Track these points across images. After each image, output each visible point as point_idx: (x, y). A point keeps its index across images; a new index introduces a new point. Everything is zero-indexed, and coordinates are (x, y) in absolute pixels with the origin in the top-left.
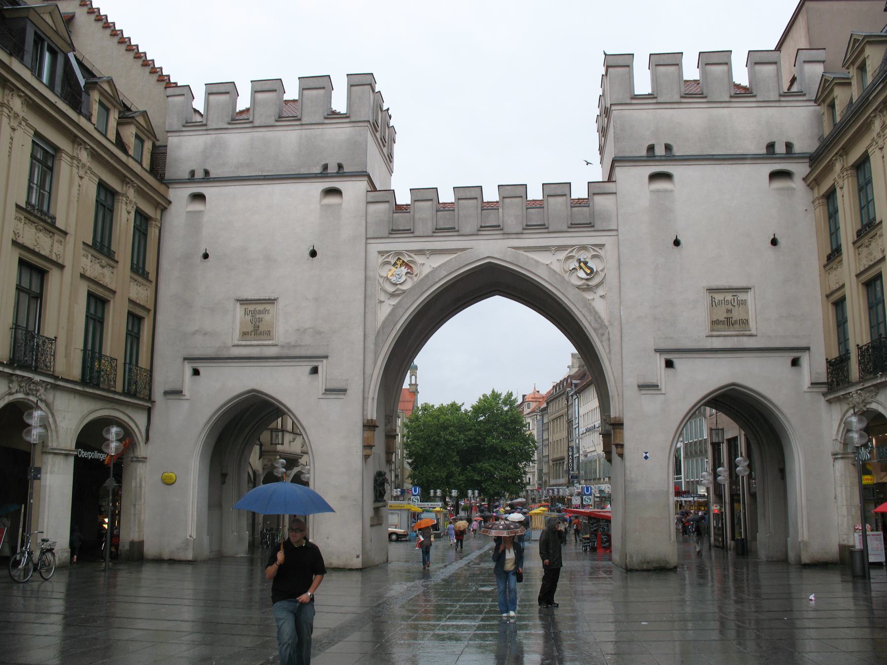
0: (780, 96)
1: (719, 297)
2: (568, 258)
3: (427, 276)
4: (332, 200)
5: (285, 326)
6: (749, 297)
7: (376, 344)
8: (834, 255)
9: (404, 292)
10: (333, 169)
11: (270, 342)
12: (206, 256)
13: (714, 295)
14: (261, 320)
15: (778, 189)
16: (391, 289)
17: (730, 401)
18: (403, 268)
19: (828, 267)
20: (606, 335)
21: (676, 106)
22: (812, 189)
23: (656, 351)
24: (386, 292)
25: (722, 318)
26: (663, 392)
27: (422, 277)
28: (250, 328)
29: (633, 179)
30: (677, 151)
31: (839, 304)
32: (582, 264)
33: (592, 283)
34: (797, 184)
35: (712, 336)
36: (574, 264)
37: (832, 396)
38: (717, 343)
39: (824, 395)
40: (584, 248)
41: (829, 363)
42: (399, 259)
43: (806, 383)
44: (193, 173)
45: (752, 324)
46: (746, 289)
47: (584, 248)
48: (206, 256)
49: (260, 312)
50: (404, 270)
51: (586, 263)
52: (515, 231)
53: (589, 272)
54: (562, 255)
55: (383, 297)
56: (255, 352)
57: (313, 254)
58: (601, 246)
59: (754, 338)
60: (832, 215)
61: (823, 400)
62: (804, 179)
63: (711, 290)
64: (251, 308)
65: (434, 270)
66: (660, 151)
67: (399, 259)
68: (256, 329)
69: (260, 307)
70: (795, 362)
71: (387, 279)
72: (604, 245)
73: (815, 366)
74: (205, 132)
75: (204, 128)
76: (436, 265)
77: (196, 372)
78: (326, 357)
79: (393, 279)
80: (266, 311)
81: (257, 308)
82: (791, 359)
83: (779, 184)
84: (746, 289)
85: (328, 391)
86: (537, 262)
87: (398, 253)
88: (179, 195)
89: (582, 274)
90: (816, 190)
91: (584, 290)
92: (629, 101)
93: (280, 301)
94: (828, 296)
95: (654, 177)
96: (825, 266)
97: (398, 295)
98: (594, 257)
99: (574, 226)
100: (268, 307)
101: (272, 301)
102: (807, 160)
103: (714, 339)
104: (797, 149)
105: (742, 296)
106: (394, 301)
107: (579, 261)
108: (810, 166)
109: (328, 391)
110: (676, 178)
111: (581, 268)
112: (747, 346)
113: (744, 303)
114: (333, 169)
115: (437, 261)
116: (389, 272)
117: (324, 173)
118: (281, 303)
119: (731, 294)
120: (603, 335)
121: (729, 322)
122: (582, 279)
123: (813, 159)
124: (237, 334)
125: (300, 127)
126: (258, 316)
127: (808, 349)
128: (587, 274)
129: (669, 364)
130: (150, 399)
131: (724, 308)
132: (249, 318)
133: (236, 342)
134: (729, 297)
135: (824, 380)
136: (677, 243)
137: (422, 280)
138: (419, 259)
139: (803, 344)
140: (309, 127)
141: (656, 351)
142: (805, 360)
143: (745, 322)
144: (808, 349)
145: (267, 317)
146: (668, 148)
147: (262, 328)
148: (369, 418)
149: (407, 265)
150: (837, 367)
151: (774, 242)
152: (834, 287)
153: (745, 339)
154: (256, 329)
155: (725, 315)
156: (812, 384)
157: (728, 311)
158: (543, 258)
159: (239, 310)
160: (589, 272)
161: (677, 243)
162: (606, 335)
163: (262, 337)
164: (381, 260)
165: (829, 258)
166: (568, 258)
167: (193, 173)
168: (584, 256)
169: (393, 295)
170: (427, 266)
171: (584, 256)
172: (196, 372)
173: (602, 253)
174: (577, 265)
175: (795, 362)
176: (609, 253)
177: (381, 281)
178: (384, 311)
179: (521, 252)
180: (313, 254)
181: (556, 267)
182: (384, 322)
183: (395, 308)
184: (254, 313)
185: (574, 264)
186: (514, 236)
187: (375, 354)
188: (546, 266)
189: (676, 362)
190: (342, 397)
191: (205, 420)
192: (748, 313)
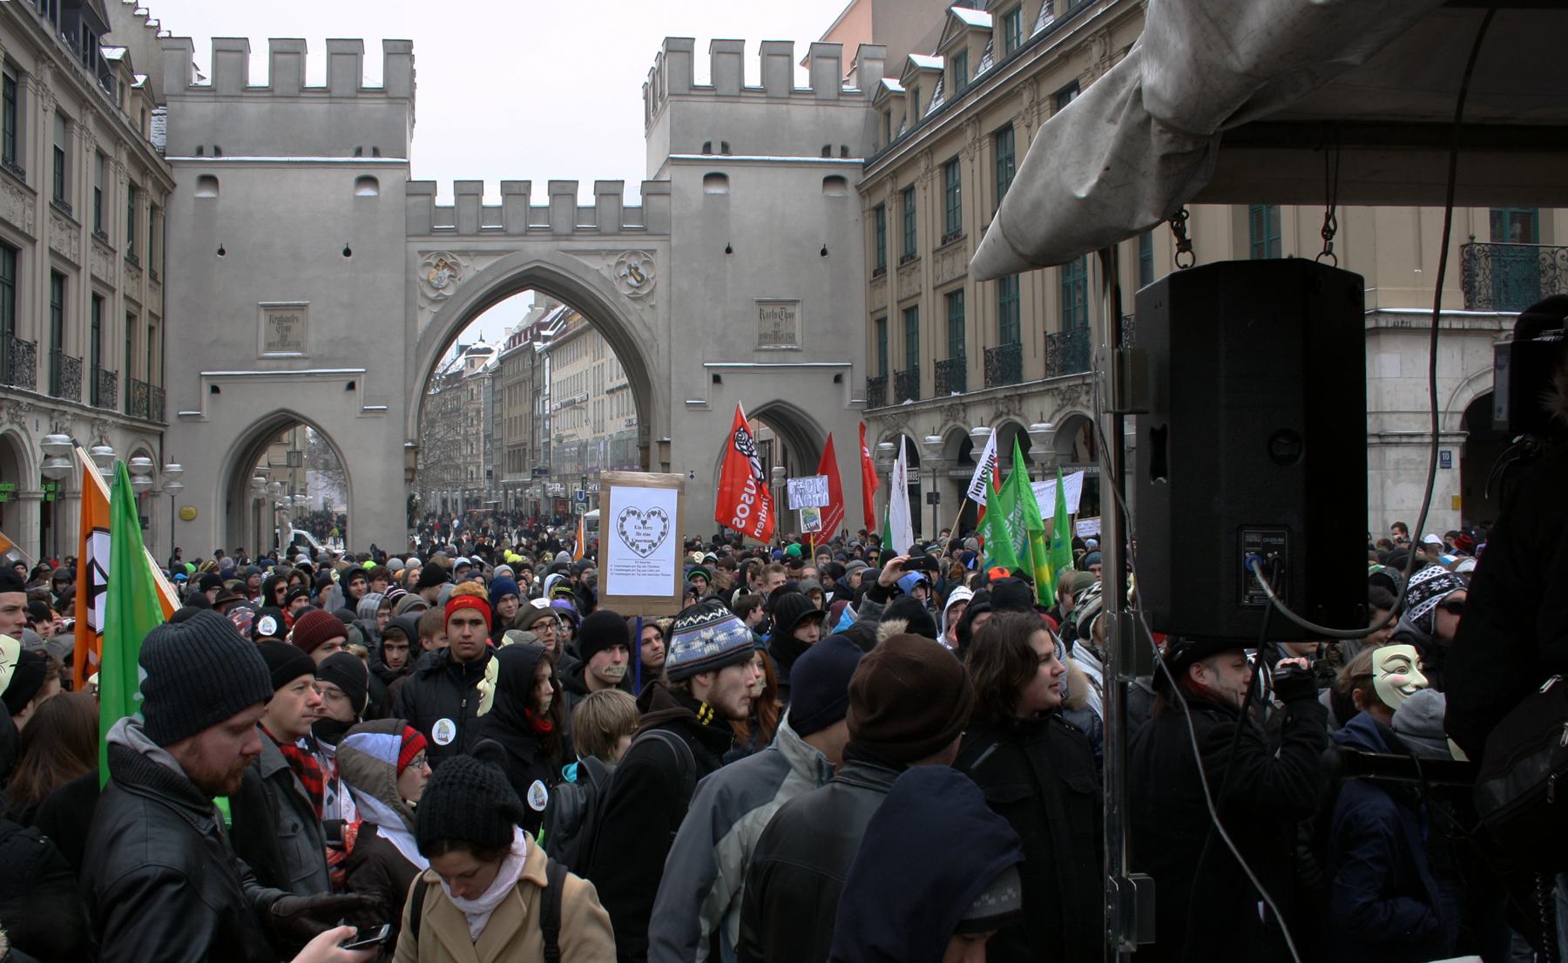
2: (619, 263)
3: (471, 281)
6: (797, 310)
8: (880, 271)
9: (447, 298)
14: (288, 329)
16: (432, 295)
17: (774, 414)
24: (424, 295)
28: (276, 338)
29: (690, 182)
31: (882, 323)
36: (624, 271)
45: (798, 338)
47: (634, 253)
49: (287, 319)
50: (447, 272)
51: (636, 269)
54: (613, 261)
55: (424, 303)
58: (653, 252)
60: (881, 230)
63: (760, 302)
64: (277, 314)
65: (480, 274)
69: (287, 314)
70: (838, 379)
71: (429, 282)
73: (856, 383)
76: (481, 268)
80: (293, 319)
84: (794, 302)
86: (586, 267)
87: (440, 254)
89: (633, 282)
91: (634, 299)
98: (644, 262)
100: (297, 314)
101: (302, 307)
105: (790, 309)
106: (436, 309)
107: (630, 267)
113: (792, 316)
115: (483, 264)
116: (433, 274)
118: (312, 310)
121: (776, 337)
124: (262, 345)
129: (717, 379)
134: (777, 310)
138: (463, 261)
142: (847, 379)
147: (292, 337)
149: (446, 265)
150: (876, 388)
152: (879, 306)
157: (776, 324)
158: (593, 263)
159: (263, 317)
161: (729, 250)
164: (421, 261)
166: (619, 263)
168: (634, 261)
169: (434, 301)
170: (472, 269)
171: (634, 261)
175: (838, 379)
176: (660, 260)
178: (424, 320)
181: (605, 273)
184: (281, 320)
185: (624, 271)
188: (598, 270)
189: (723, 377)
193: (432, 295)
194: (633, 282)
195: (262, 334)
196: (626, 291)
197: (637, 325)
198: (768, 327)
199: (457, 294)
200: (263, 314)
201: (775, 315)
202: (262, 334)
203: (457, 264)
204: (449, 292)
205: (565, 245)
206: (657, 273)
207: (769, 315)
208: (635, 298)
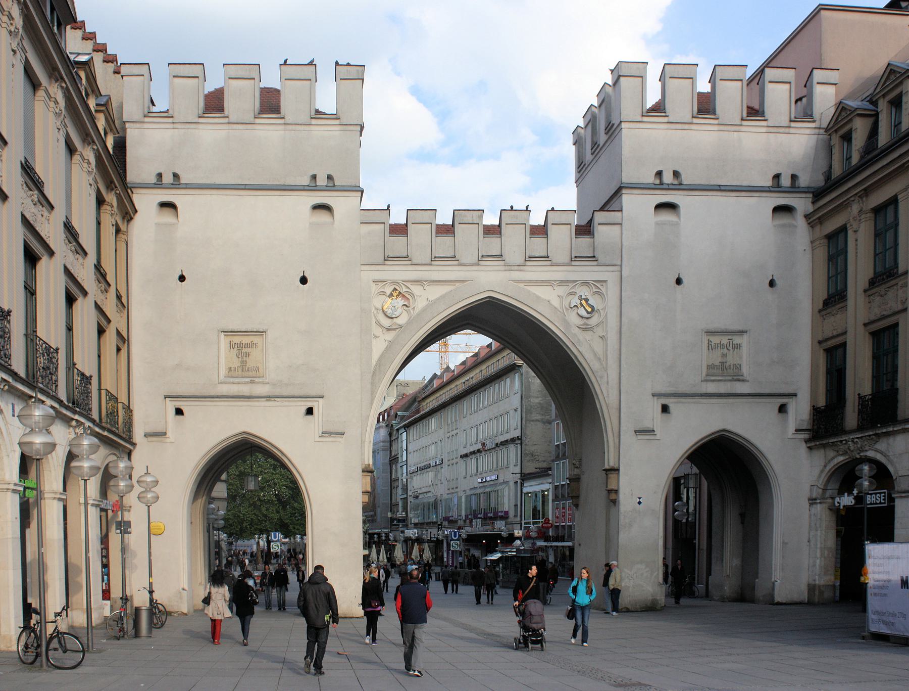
0: (791, 121)
1: (715, 340)
3: (424, 310)
4: (323, 216)
5: (275, 362)
6: (743, 340)
7: (372, 384)
8: (834, 299)
10: (322, 181)
11: (260, 380)
12: (182, 278)
13: (711, 338)
15: (784, 226)
18: (399, 299)
19: (824, 313)
20: (605, 379)
21: (686, 126)
22: (812, 227)
23: (654, 395)
24: (381, 326)
25: (717, 363)
26: (658, 437)
27: (417, 311)
28: (236, 363)
30: (686, 180)
32: (583, 302)
33: (594, 321)
34: (800, 222)
35: (707, 381)
36: (575, 301)
37: (813, 444)
38: (711, 388)
39: (806, 442)
40: (585, 283)
41: (816, 410)
42: (395, 289)
43: (791, 428)
44: (160, 175)
45: (745, 370)
46: (742, 332)
47: (585, 283)
48: (182, 278)
50: (400, 302)
51: (587, 300)
52: (518, 262)
53: (590, 310)
55: (377, 331)
56: (245, 390)
57: (304, 280)
59: (747, 383)
61: (803, 446)
62: (807, 217)
63: (709, 332)
64: (237, 340)
65: (432, 304)
66: (668, 178)
67: (395, 289)
68: (244, 363)
69: (246, 340)
70: (782, 409)
72: (605, 282)
74: (171, 126)
75: (170, 120)
76: (433, 297)
77: (179, 412)
78: (322, 397)
79: (389, 312)
80: (251, 345)
81: (243, 341)
82: (778, 405)
83: (784, 219)
85: (326, 434)
86: (538, 298)
88: (146, 203)
89: (582, 312)
90: (818, 228)
91: (585, 330)
92: (640, 119)
93: (269, 333)
94: (820, 342)
95: (660, 207)
96: (820, 311)
97: (394, 329)
99: (575, 259)
101: (261, 333)
102: (811, 195)
103: (710, 384)
104: (803, 181)
105: (737, 340)
106: (390, 336)
107: (581, 299)
108: (813, 203)
109: (326, 434)
110: (682, 210)
111: (582, 305)
112: (739, 391)
113: (738, 347)
114: (322, 181)
117: (312, 186)
119: (727, 338)
120: (601, 377)
122: (582, 317)
123: (817, 194)
124: (223, 372)
125: (282, 127)
126: (244, 350)
127: (795, 395)
128: (588, 313)
130: (130, 440)
131: (719, 352)
132: (235, 351)
133: (222, 378)
134: (725, 340)
135: (809, 427)
136: (679, 281)
137: (418, 315)
138: (416, 290)
139: (790, 390)
140: (294, 127)
141: (654, 395)
142: (791, 409)
143: (739, 367)
144: (795, 395)
145: (255, 354)
146: (676, 174)
147: (251, 363)
148: (367, 463)
151: (772, 284)
153: (738, 384)
154: (244, 363)
155: (720, 359)
156: (796, 430)
160: (590, 310)
162: (605, 379)
163: (250, 374)
164: (374, 288)
165: (827, 303)
167: (160, 175)
168: (584, 292)
170: (423, 296)
172: (179, 412)
173: (604, 290)
174: (578, 302)
175: (782, 409)
177: (375, 312)
179: (522, 285)
180: (304, 280)
181: (556, 303)
182: (379, 360)
183: (391, 344)
184: (240, 346)
185: (575, 301)
186: (516, 268)
187: (372, 394)
189: (672, 407)
190: (340, 440)
191: (193, 464)
192: (741, 358)
193: (386, 322)
194: (584, 314)
195: (223, 361)
196: (579, 322)
197: (588, 355)
198: (716, 358)
199: (409, 323)
200: (224, 341)
201: (722, 346)
202: (223, 361)
203: (412, 294)
204: (402, 320)
205: (517, 275)
206: (608, 306)
207: (717, 346)
208: (586, 329)
